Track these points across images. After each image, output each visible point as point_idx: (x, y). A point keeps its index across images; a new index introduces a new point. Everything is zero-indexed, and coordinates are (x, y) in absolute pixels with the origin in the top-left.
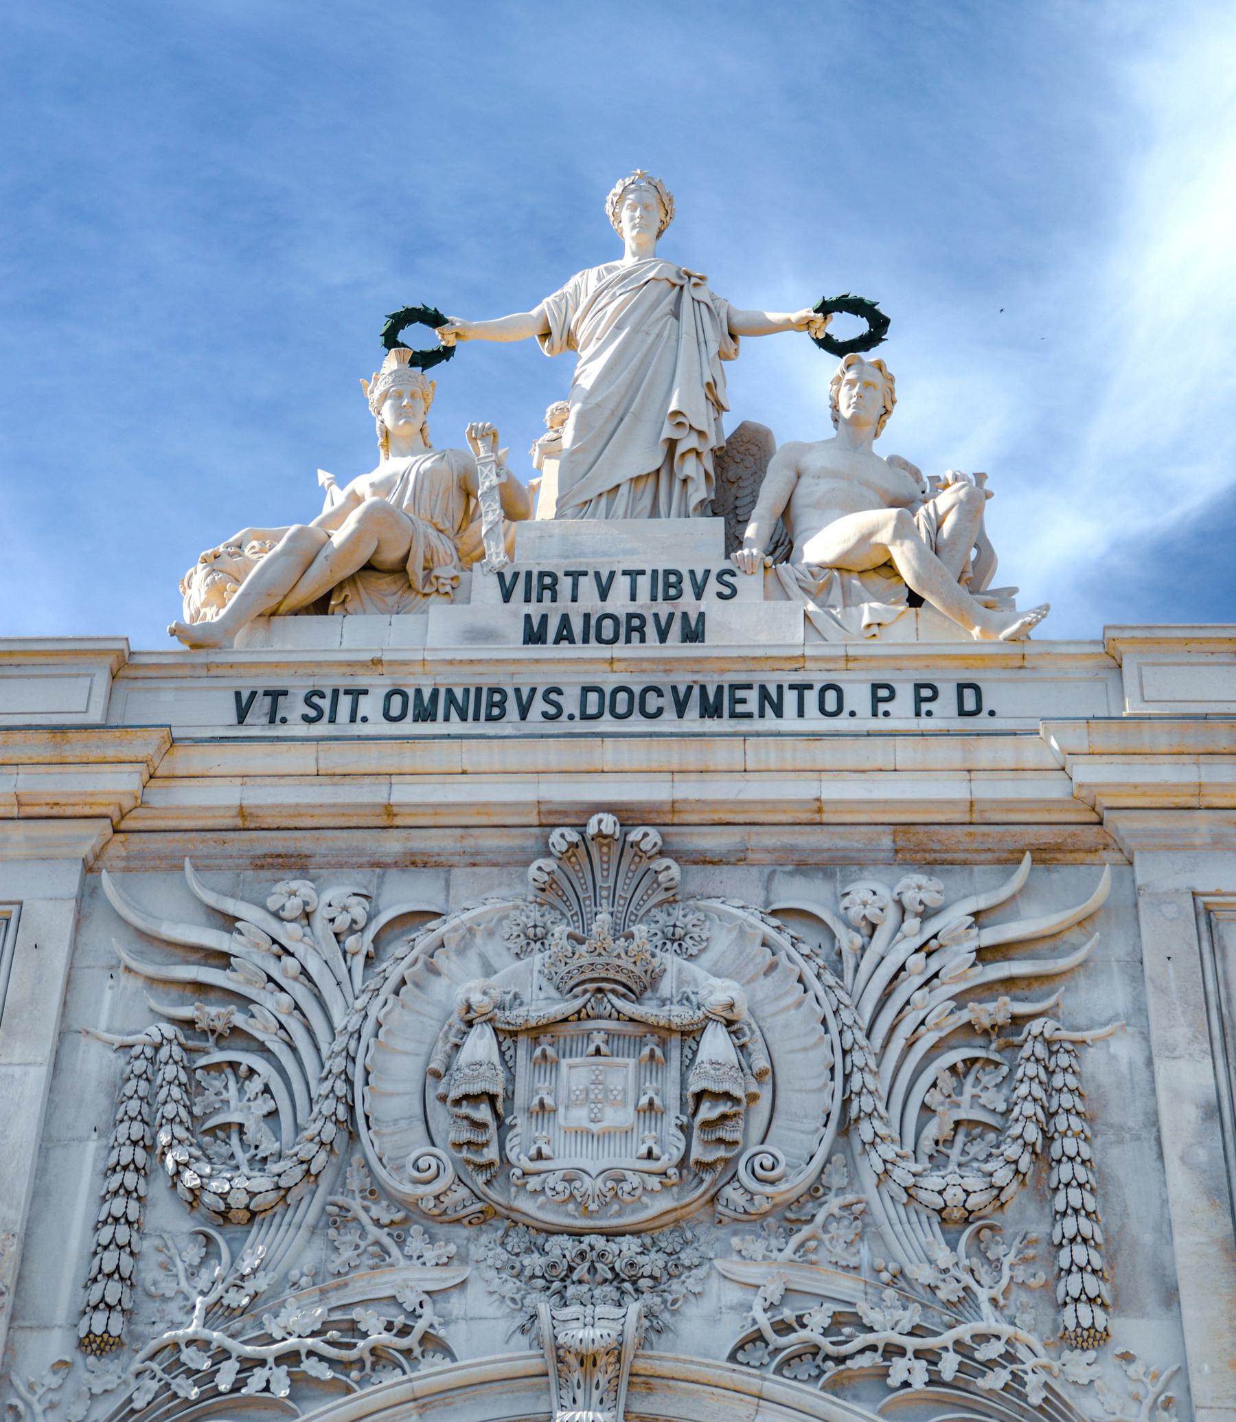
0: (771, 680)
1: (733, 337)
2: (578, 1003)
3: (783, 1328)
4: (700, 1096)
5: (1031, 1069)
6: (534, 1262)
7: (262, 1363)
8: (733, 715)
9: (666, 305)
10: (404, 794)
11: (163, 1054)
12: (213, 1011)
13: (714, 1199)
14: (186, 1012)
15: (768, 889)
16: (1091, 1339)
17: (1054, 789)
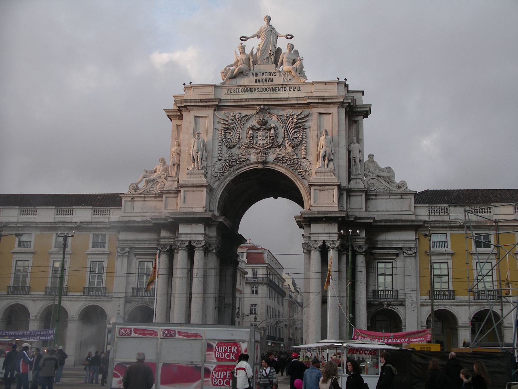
0: (279, 86)
1: (277, 36)
2: (260, 127)
3: (278, 158)
4: (271, 136)
5: (301, 132)
6: (256, 151)
7: (233, 162)
8: (276, 91)
9: (270, 34)
11: (223, 131)
12: (227, 126)
13: (272, 145)
14: (224, 127)
15: (278, 112)
16: (305, 158)
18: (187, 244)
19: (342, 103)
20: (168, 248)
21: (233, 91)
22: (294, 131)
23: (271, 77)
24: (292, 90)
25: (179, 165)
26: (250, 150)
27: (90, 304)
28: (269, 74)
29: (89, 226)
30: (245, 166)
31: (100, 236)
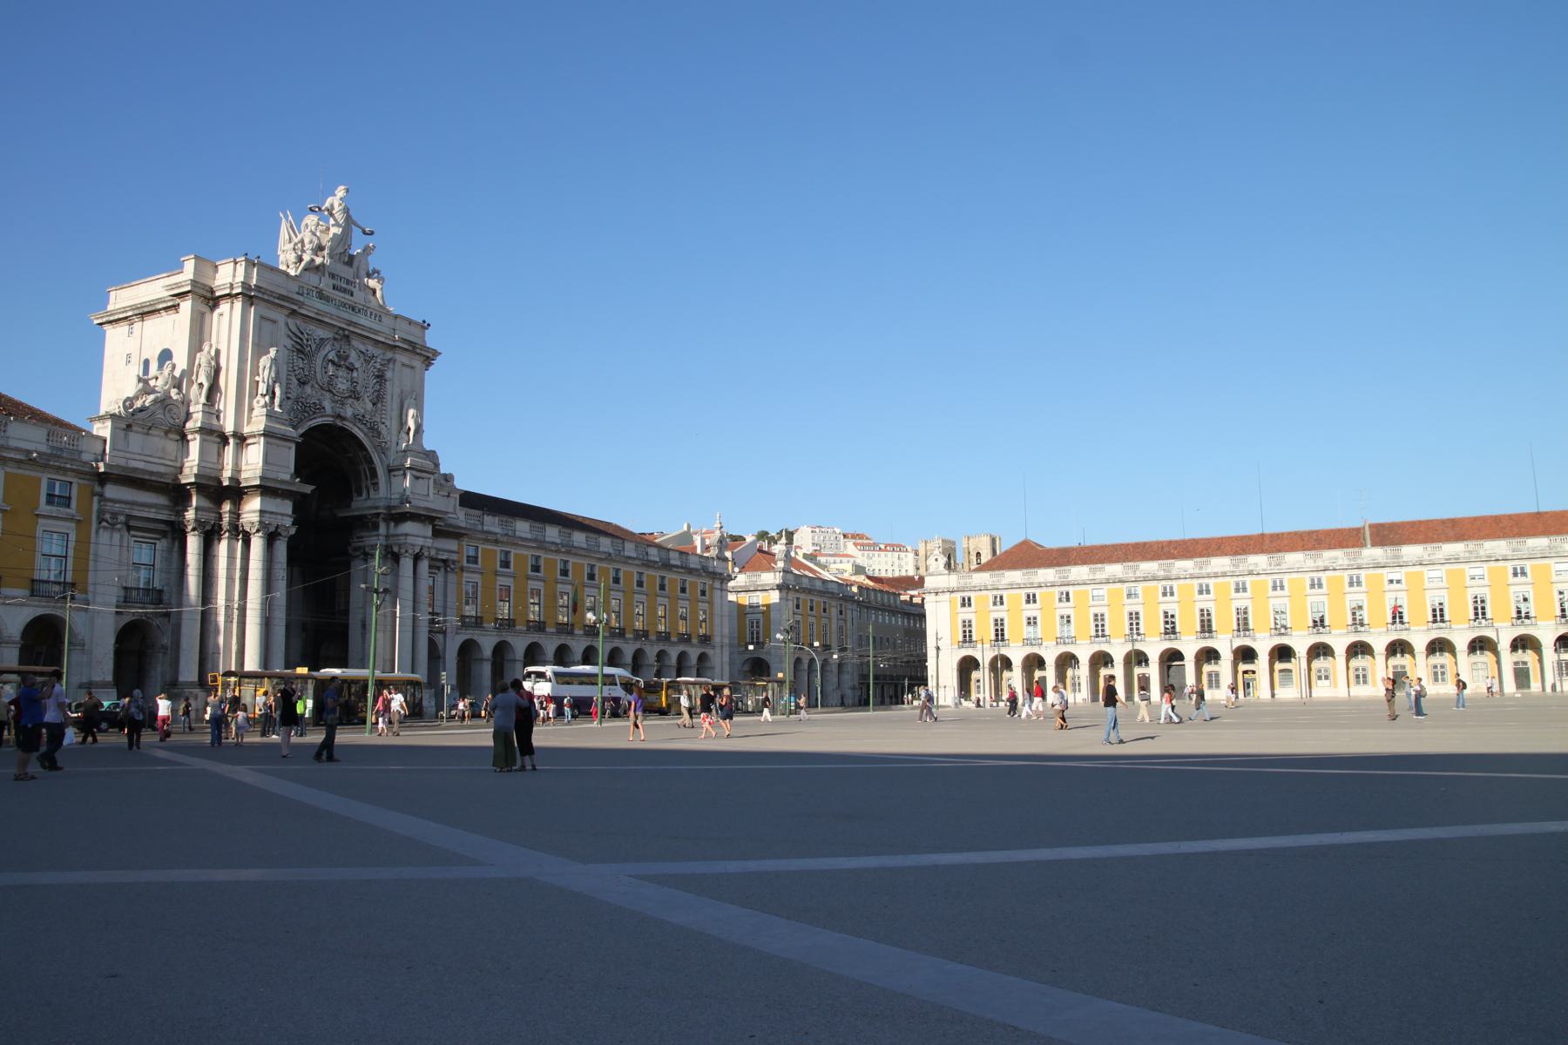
10: (326, 320)
14: (299, 347)
16: (383, 423)
17: (392, 343)
18: (272, 529)
19: (428, 357)
20: (208, 528)
21: (306, 292)
22: (375, 381)
23: (349, 287)
24: (373, 317)
25: (213, 390)
26: (324, 392)
27: (44, 613)
28: (348, 282)
29: (51, 463)
30: (320, 417)
31: (58, 484)
